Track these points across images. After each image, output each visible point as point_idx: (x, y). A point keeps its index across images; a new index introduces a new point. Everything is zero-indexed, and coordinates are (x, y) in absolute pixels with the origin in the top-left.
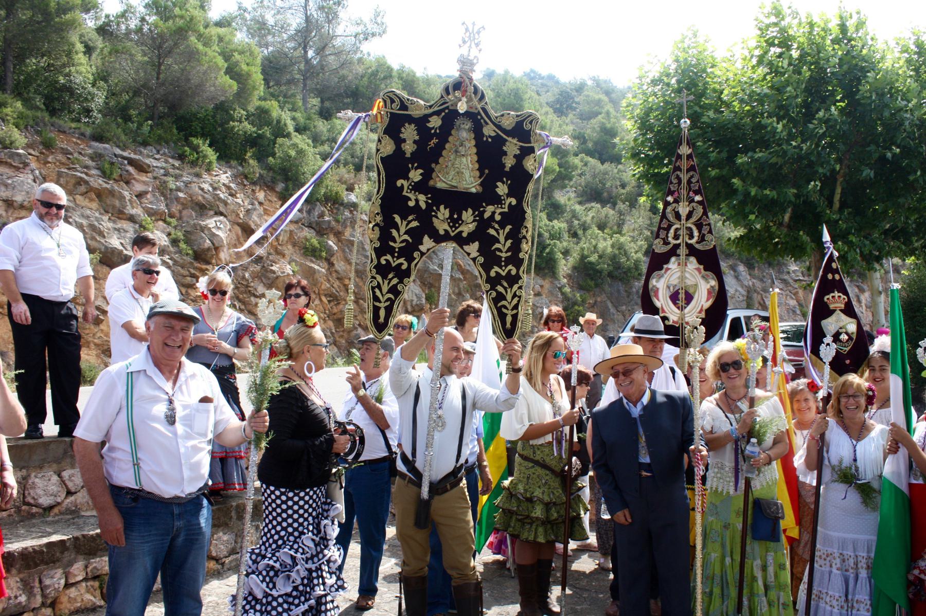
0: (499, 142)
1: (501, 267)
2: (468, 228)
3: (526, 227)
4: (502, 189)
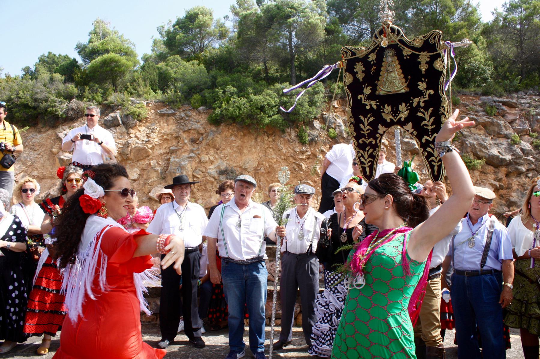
1: (428, 136)
2: (403, 115)
3: (443, 107)
4: (422, 86)
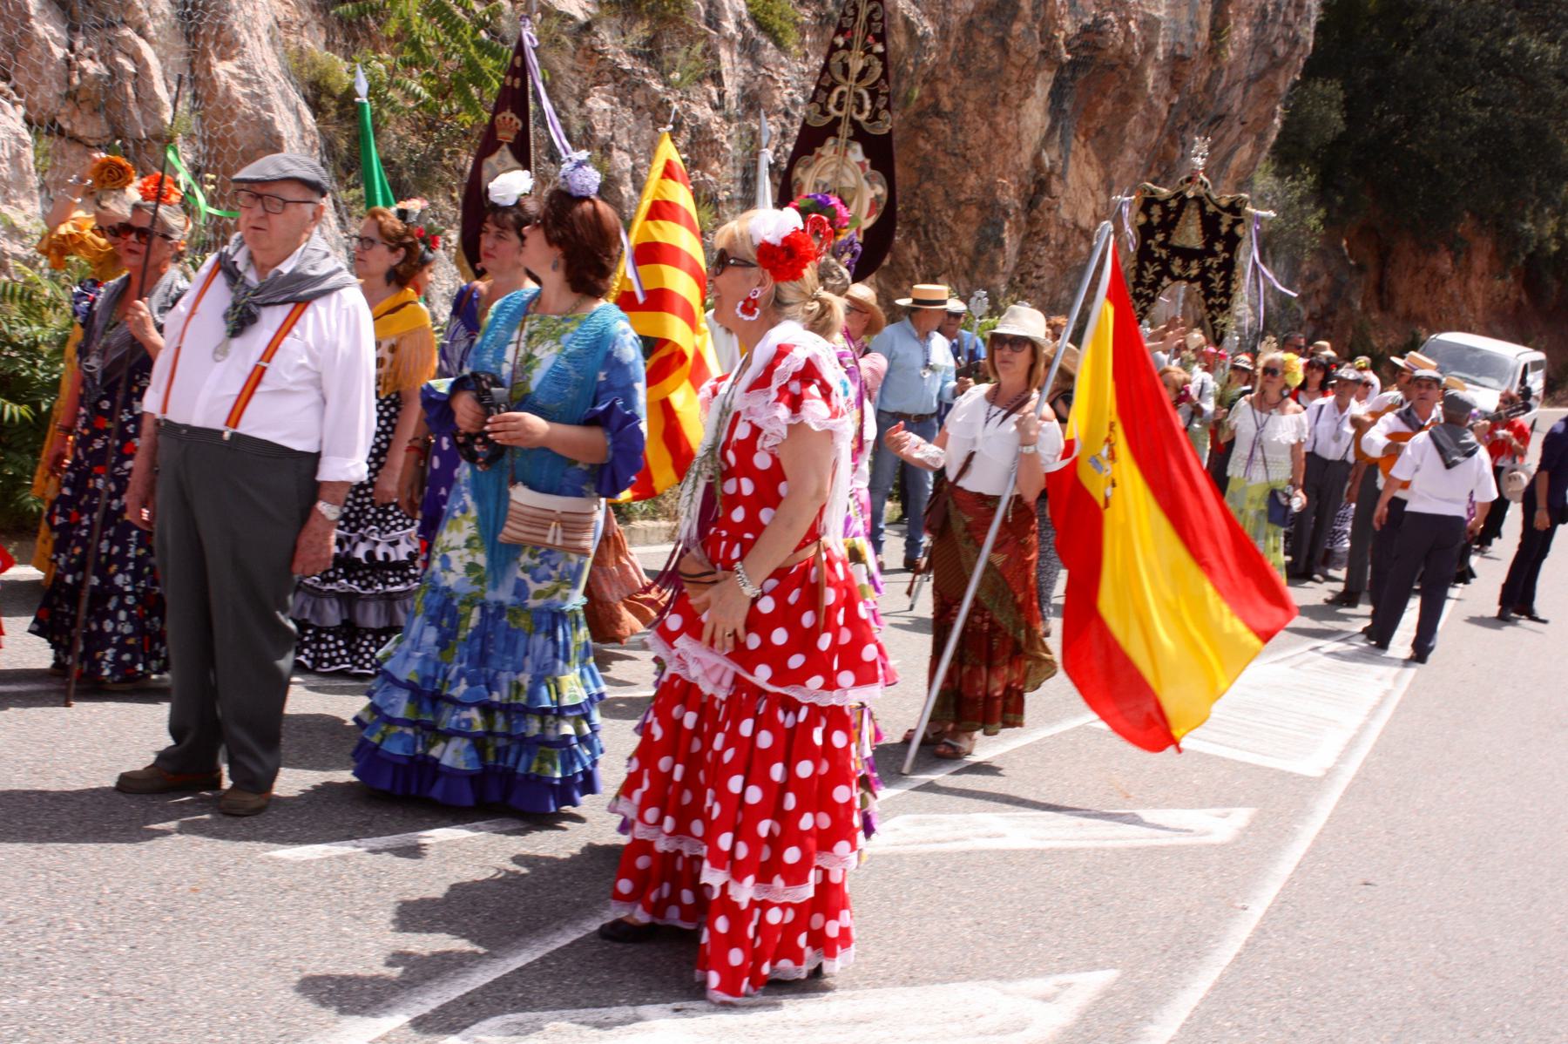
0: (1217, 216)
2: (1194, 272)
4: (1218, 247)
